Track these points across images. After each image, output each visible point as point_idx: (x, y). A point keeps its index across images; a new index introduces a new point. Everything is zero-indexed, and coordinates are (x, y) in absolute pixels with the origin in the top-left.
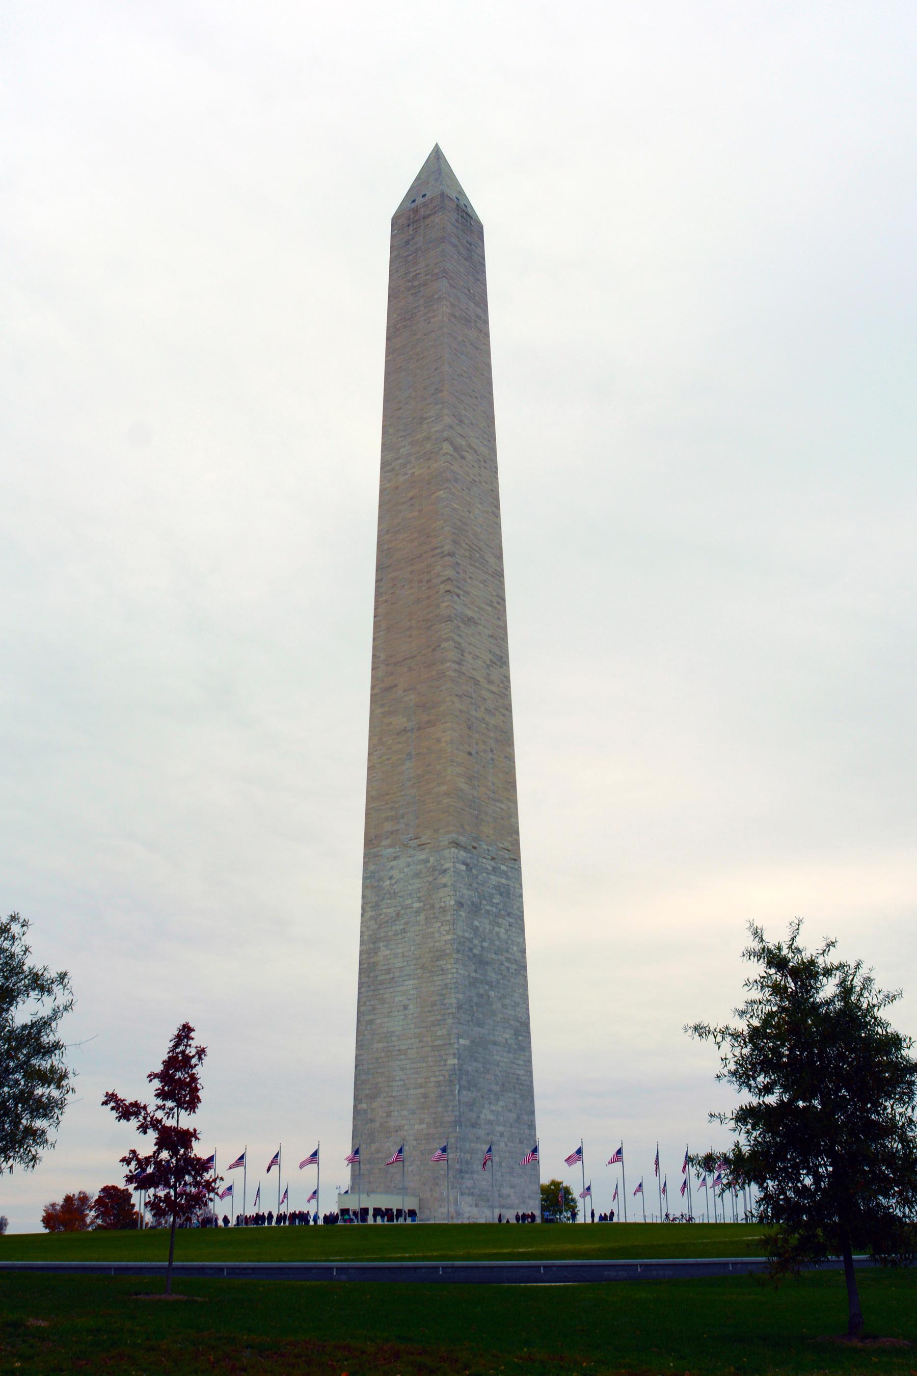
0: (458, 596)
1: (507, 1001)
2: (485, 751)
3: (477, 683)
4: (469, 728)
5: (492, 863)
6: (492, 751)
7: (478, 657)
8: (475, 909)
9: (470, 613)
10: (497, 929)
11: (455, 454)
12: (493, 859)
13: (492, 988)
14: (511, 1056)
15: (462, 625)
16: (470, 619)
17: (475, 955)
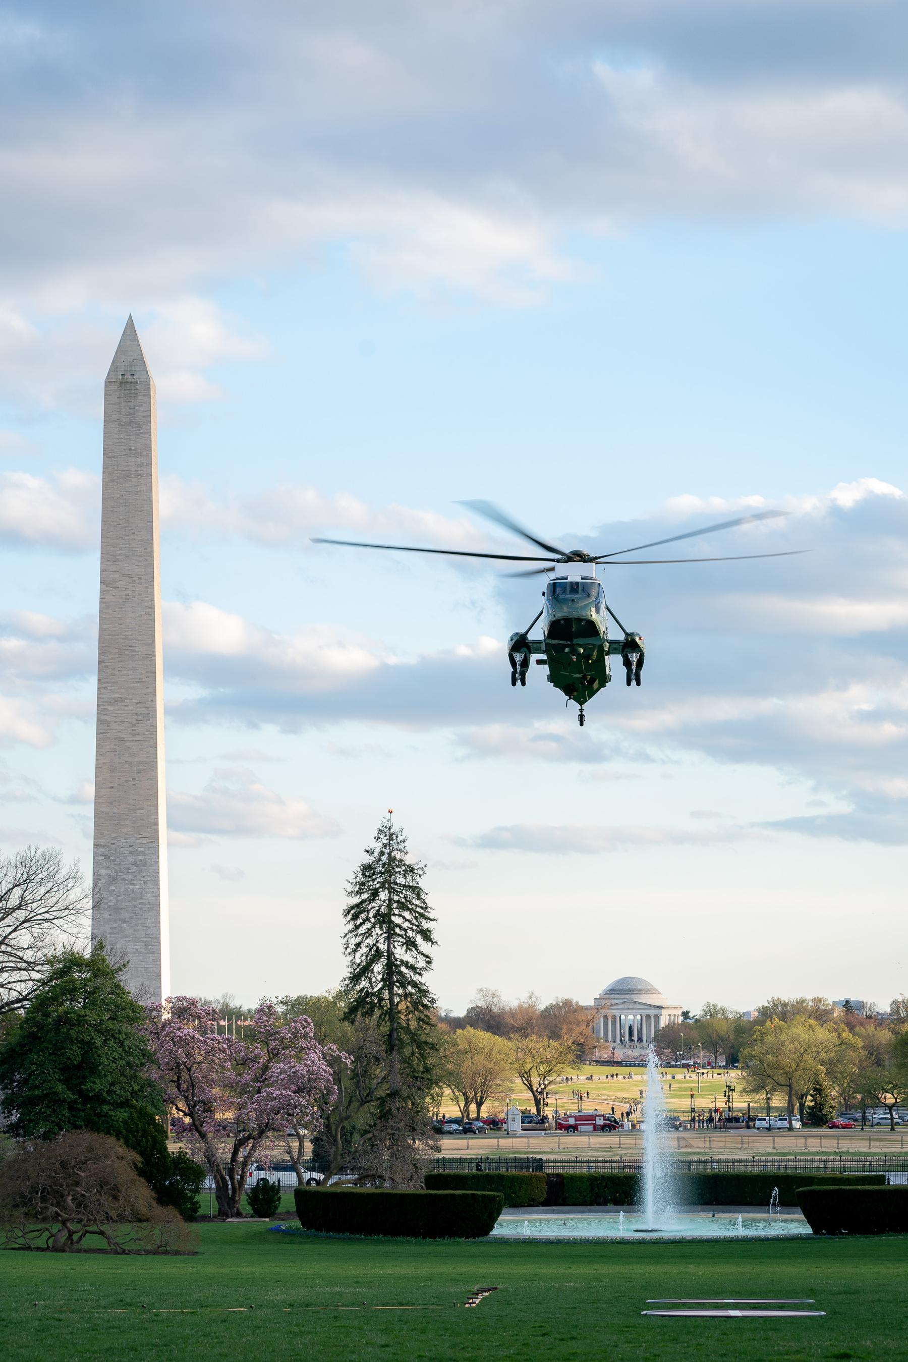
0: (106, 688)
1: (140, 927)
2: (127, 782)
3: (121, 740)
4: (112, 771)
5: (130, 849)
6: (134, 779)
7: (123, 722)
8: (113, 880)
9: (117, 696)
10: (132, 887)
11: (108, 589)
12: (131, 846)
13: (124, 921)
14: (141, 958)
15: (109, 708)
16: (116, 700)
17: (110, 906)
